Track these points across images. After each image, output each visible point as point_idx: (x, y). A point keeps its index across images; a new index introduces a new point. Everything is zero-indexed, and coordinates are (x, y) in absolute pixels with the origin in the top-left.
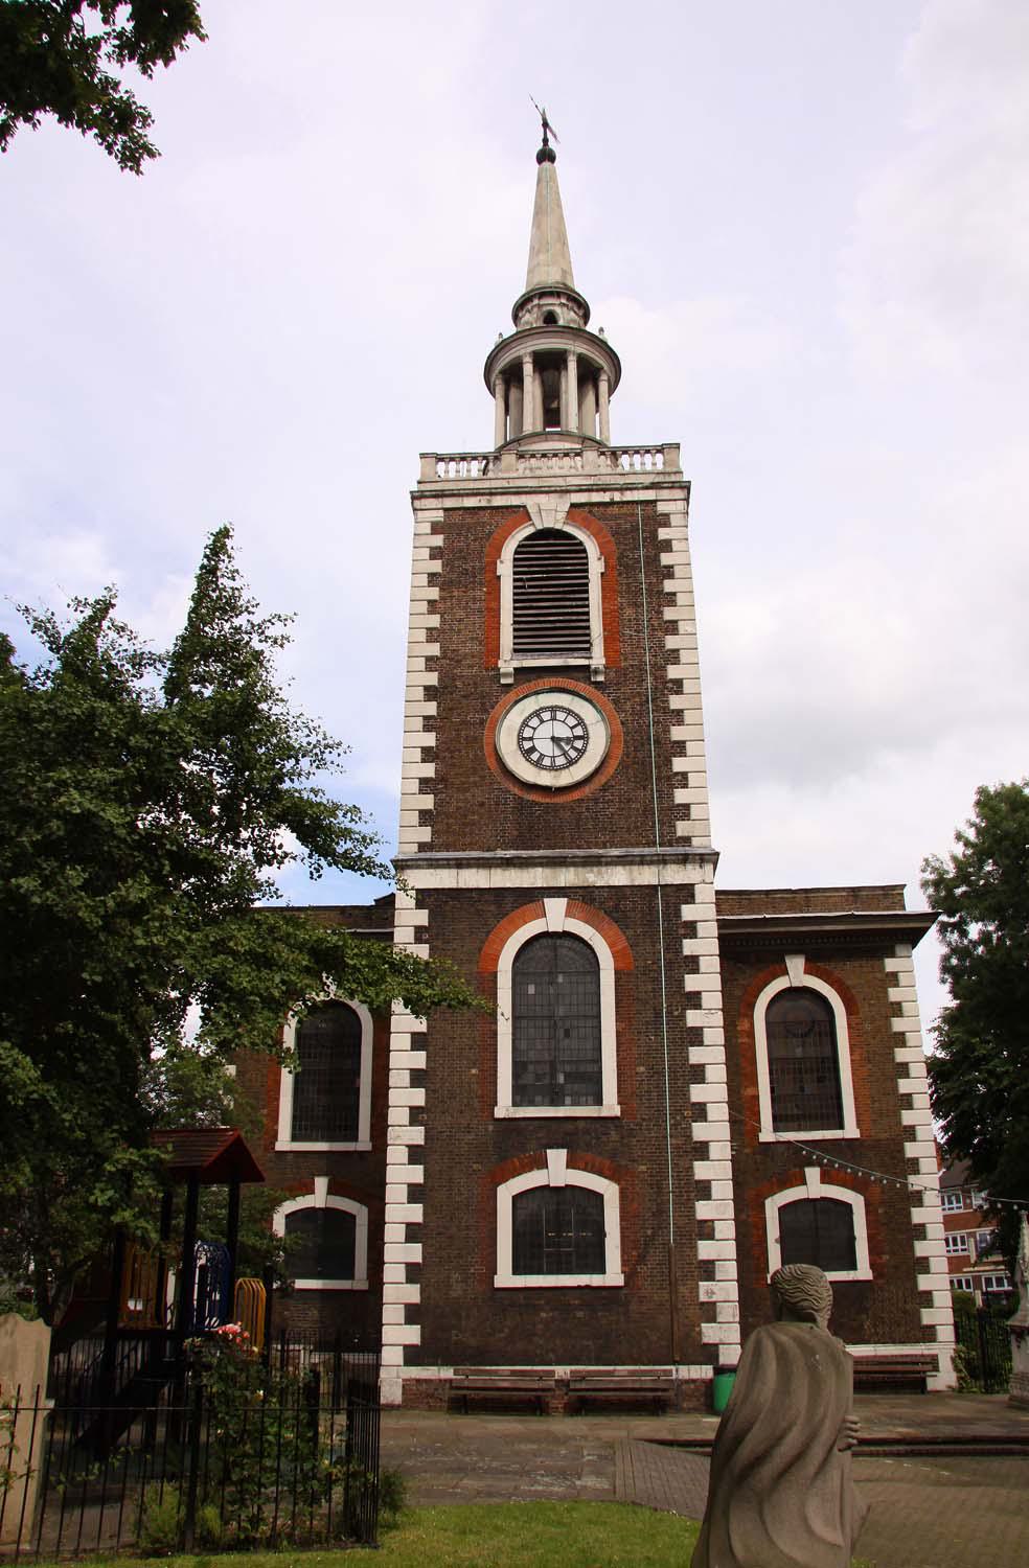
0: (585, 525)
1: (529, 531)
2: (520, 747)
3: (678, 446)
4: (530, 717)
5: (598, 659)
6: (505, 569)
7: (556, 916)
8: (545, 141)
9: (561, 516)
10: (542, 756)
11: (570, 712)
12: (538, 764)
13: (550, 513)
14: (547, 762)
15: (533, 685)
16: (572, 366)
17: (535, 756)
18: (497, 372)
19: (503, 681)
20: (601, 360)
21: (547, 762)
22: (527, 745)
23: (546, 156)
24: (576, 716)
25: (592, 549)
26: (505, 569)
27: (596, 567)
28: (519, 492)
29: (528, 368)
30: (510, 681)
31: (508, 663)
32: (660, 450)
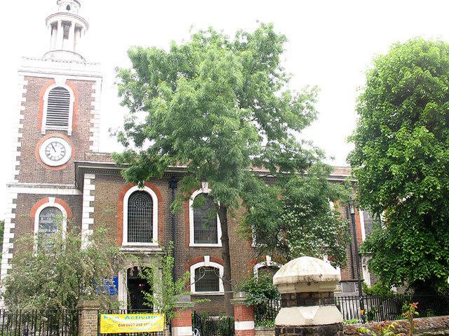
1: (55, 87)
5: (70, 129)
7: (52, 202)
13: (60, 82)
20: (83, 25)
29: (59, 25)
30: (44, 133)
31: (44, 128)
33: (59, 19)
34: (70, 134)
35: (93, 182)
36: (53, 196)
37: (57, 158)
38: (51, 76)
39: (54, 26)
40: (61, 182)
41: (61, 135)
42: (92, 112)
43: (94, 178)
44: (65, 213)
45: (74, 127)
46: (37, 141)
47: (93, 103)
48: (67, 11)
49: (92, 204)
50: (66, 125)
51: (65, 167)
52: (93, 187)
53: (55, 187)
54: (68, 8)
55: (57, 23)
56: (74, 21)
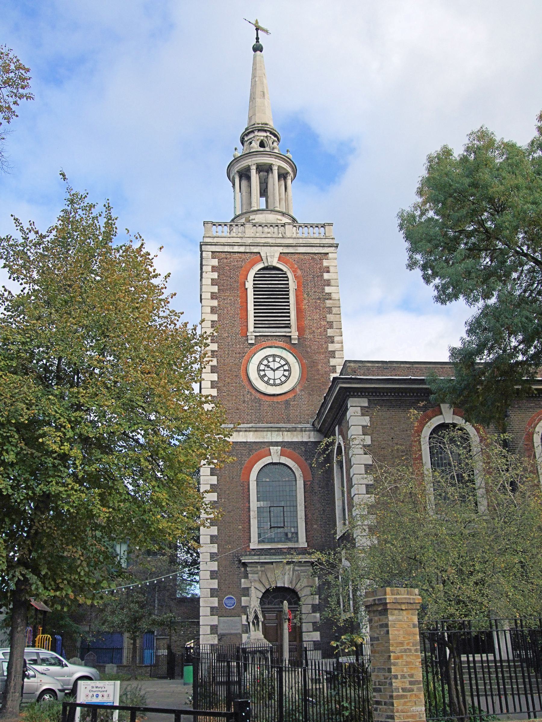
0: (286, 263)
1: (261, 266)
2: (259, 374)
3: (331, 225)
4: (263, 360)
5: (294, 334)
6: (250, 285)
8: (257, 39)
9: (276, 260)
10: (269, 379)
11: (282, 358)
12: (267, 383)
14: (271, 382)
15: (264, 344)
16: (276, 172)
17: (266, 379)
18: (236, 170)
19: (250, 342)
20: (289, 170)
21: (271, 382)
22: (262, 373)
23: (257, 48)
24: (285, 360)
25: (290, 275)
26: (250, 285)
27: (292, 285)
28: (257, 245)
29: (253, 172)
30: (253, 342)
32: (323, 226)
33: (252, 162)
34: (296, 342)
35: (364, 411)
36: (276, 444)
37: (278, 382)
38: (255, 249)
39: (245, 175)
40: (289, 422)
41: (281, 344)
42: (328, 303)
43: (366, 405)
44: (298, 473)
45: (300, 329)
46: (242, 354)
47: (327, 289)
48: (262, 149)
49: (367, 449)
50: (288, 326)
51: (291, 396)
52: (366, 421)
53: (279, 430)
54: (262, 145)
55: (248, 169)
56: (277, 163)
